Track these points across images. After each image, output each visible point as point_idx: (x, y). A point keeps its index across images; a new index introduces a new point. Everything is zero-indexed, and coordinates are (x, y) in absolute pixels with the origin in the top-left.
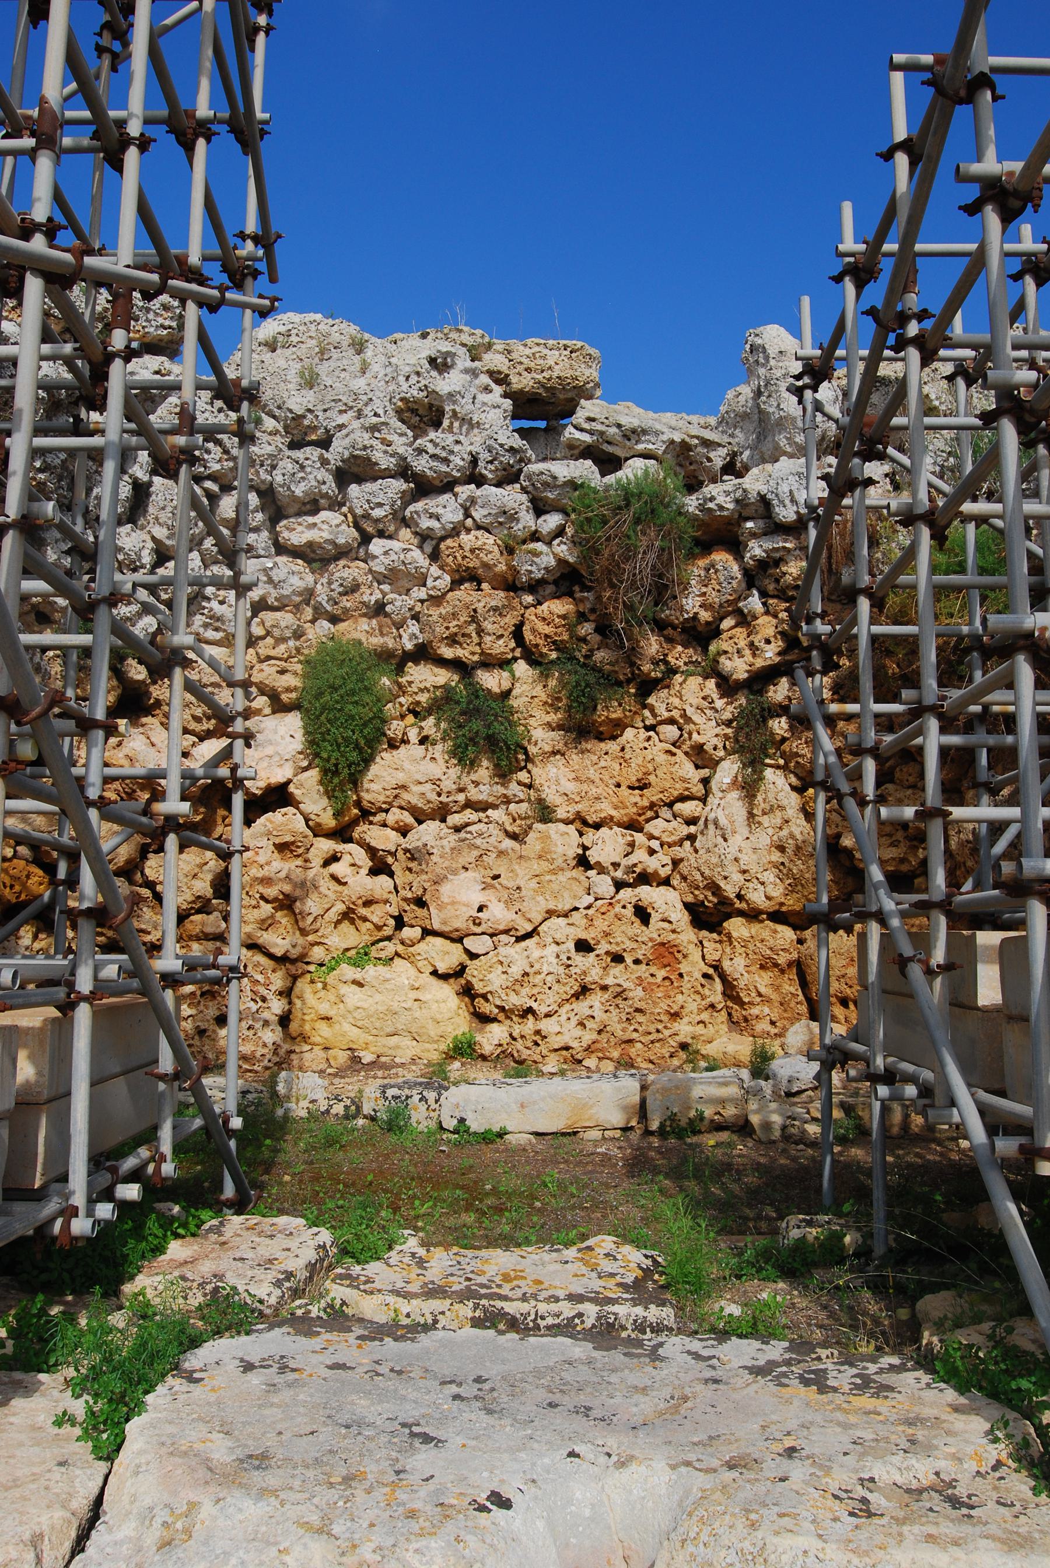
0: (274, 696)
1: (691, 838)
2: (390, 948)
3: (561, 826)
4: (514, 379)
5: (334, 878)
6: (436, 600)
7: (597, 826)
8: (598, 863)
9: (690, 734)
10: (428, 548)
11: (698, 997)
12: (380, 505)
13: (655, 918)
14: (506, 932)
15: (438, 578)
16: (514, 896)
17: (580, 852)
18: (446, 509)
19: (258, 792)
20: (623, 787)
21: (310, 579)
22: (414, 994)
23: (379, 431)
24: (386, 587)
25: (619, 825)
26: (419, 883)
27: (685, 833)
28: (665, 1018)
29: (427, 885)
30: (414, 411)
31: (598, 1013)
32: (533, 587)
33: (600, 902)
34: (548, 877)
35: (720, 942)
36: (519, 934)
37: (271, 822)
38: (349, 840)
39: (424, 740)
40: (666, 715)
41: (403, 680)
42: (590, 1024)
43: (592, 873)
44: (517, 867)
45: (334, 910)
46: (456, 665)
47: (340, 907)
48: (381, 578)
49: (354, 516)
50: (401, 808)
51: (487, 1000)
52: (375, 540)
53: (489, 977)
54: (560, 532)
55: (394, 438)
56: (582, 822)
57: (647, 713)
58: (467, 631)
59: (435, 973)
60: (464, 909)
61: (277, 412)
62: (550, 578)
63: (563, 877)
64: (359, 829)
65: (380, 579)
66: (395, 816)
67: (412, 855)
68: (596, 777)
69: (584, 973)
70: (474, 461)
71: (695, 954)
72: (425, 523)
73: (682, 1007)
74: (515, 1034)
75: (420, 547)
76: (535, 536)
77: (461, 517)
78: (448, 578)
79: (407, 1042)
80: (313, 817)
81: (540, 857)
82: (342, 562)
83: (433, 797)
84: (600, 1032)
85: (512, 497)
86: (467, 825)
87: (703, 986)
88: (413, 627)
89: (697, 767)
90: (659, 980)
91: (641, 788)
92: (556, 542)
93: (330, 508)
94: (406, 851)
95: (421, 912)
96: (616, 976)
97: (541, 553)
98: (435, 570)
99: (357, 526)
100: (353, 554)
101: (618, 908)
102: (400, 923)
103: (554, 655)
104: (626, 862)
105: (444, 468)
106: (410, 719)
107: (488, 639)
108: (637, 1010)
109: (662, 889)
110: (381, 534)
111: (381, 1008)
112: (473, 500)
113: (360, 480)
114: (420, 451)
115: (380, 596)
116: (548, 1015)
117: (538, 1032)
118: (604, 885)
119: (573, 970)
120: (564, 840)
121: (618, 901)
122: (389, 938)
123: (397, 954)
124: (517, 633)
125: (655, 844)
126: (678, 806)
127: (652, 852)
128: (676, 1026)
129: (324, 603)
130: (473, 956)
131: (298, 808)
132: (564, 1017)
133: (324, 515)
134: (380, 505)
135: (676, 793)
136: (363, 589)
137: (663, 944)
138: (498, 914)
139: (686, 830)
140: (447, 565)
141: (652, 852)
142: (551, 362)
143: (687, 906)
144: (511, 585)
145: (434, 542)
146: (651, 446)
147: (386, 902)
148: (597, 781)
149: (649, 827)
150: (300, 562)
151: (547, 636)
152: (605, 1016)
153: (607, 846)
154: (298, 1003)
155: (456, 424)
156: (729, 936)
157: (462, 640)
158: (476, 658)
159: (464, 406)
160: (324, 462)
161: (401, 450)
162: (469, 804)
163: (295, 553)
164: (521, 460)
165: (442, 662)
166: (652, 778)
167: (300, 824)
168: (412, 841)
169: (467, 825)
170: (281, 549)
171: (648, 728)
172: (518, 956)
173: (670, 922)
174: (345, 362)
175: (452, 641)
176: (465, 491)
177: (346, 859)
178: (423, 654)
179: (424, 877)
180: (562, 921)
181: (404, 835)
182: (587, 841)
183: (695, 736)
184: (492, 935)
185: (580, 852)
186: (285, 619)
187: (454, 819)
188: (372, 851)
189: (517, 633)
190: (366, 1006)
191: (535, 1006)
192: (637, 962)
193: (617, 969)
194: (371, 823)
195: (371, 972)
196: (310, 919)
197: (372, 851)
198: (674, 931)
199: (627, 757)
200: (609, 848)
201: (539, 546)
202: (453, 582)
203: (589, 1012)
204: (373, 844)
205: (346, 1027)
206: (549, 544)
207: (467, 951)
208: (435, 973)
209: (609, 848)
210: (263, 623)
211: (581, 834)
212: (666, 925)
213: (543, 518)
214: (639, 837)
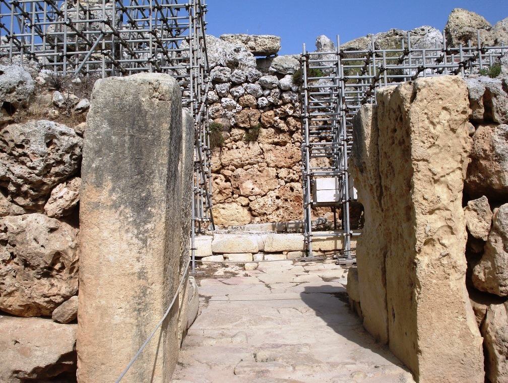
2: (231, 200)
5: (216, 183)
6: (238, 113)
7: (281, 168)
8: (281, 177)
10: (236, 99)
12: (224, 90)
14: (259, 195)
16: (260, 186)
18: (240, 90)
22: (237, 211)
24: (226, 110)
26: (237, 183)
28: (298, 214)
31: (282, 214)
32: (263, 108)
38: (220, 174)
39: (237, 148)
41: (231, 133)
43: (280, 180)
46: (244, 128)
47: (218, 190)
50: (232, 165)
53: (255, 206)
54: (269, 94)
55: (227, 72)
56: (277, 167)
57: (292, 139)
64: (222, 171)
65: (224, 108)
66: (231, 167)
67: (235, 177)
68: (279, 155)
70: (247, 77)
72: (235, 94)
75: (234, 99)
76: (263, 95)
79: (235, 222)
82: (215, 104)
83: (240, 162)
84: (282, 218)
85: (256, 86)
86: (249, 169)
88: (233, 119)
94: (234, 176)
95: (238, 191)
96: (287, 205)
98: (238, 105)
99: (218, 95)
101: (286, 188)
102: (233, 194)
103: (269, 125)
106: (233, 142)
107: (252, 122)
108: (291, 212)
110: (224, 97)
112: (247, 87)
114: (233, 76)
116: (269, 214)
117: (267, 218)
118: (283, 182)
120: (273, 172)
122: (230, 197)
123: (232, 201)
124: (259, 120)
125: (295, 172)
127: (294, 174)
128: (300, 216)
130: (251, 201)
132: (273, 215)
134: (224, 90)
136: (220, 111)
138: (257, 190)
142: (266, 43)
144: (257, 107)
147: (229, 188)
149: (294, 168)
151: (267, 121)
152: (283, 214)
153: (283, 173)
155: (242, 66)
158: (249, 127)
159: (244, 61)
161: (228, 76)
162: (249, 164)
165: (241, 128)
168: (235, 173)
169: (249, 169)
171: (293, 143)
172: (261, 200)
175: (243, 122)
176: (245, 85)
177: (219, 178)
178: (236, 126)
180: (273, 192)
187: (245, 167)
188: (225, 176)
189: (259, 120)
191: (266, 212)
193: (287, 203)
194: (225, 169)
195: (226, 205)
197: (225, 176)
201: (264, 98)
204: (226, 174)
205: (221, 219)
206: (266, 97)
207: (250, 200)
208: (242, 205)
214: (291, 170)
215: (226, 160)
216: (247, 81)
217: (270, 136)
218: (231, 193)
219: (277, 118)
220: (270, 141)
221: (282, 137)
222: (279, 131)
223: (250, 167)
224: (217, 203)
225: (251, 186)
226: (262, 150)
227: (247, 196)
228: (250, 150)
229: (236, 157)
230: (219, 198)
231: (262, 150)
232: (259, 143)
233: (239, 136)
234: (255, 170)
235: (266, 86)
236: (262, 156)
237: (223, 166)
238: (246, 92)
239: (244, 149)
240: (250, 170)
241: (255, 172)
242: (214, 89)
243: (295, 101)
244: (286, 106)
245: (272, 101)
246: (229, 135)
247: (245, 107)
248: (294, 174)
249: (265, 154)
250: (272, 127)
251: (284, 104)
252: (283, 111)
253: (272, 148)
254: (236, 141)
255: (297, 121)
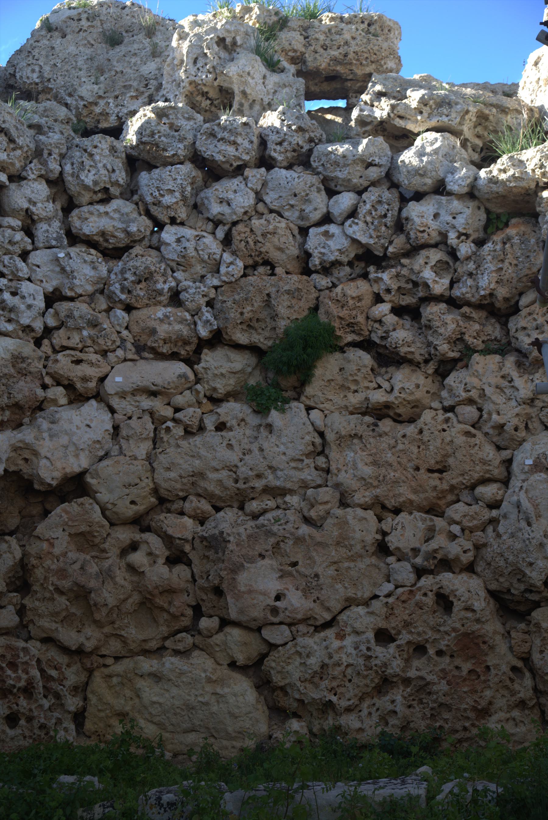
0: (70, 387)
1: (494, 521)
3: (359, 511)
4: (309, 57)
5: (132, 568)
7: (397, 511)
8: (398, 549)
9: (490, 414)
10: (221, 233)
11: (506, 693)
12: (171, 192)
13: (457, 606)
14: (305, 620)
15: (231, 263)
16: (311, 586)
17: (379, 537)
19: (54, 483)
20: (422, 471)
21: (103, 269)
23: (167, 116)
25: (420, 509)
27: (487, 517)
29: (223, 573)
30: (205, 94)
31: (399, 708)
32: (326, 269)
33: (400, 590)
34: (346, 564)
35: (527, 632)
36: (318, 623)
37: (67, 512)
38: (147, 529)
39: (221, 427)
40: (464, 395)
42: (393, 721)
43: (391, 559)
44: (314, 554)
45: (130, 601)
48: (174, 264)
49: (146, 204)
50: (199, 495)
51: (286, 694)
52: (167, 228)
53: (288, 670)
54: (353, 214)
55: (182, 122)
58: (261, 316)
59: (233, 665)
60: (261, 598)
61: (69, 100)
62: (345, 259)
63: (361, 565)
66: (194, 504)
69: (385, 665)
71: (502, 647)
72: (215, 209)
73: (490, 703)
74: (315, 730)
76: (327, 219)
77: (252, 201)
78: (240, 264)
80: (110, 506)
81: (338, 543)
83: (230, 483)
87: (512, 680)
88: (207, 315)
89: (499, 448)
90: (464, 673)
91: (440, 471)
92: (348, 223)
93: (122, 196)
94: (203, 539)
96: (418, 668)
97: (333, 235)
98: (227, 257)
99: (148, 214)
100: (146, 242)
102: (198, 611)
103: (350, 338)
104: (425, 548)
105: (231, 150)
106: (208, 405)
109: (464, 576)
110: (173, 221)
111: (177, 703)
113: (150, 167)
115: (173, 284)
116: (349, 710)
118: (404, 572)
119: (374, 662)
120: (363, 527)
121: (420, 589)
122: (185, 630)
125: (456, 529)
126: (480, 490)
129: (118, 292)
130: (273, 646)
131: (95, 499)
132: (365, 712)
133: (116, 203)
134: (171, 192)
135: (476, 476)
137: (466, 635)
138: (296, 602)
139: (488, 514)
140: (239, 250)
141: (453, 537)
143: (492, 594)
145: (226, 228)
146: (445, 119)
148: (395, 464)
150: (93, 251)
152: (408, 712)
153: (407, 531)
154: (93, 700)
156: (538, 625)
157: (256, 325)
160: (113, 150)
162: (269, 491)
163: (90, 243)
164: (311, 140)
165: (237, 347)
166: (451, 461)
167: (97, 514)
168: (210, 529)
169: (264, 512)
170: (73, 238)
172: (317, 647)
173: (473, 611)
174: (136, 46)
176: (255, 175)
177: (144, 548)
178: (217, 339)
179: (221, 565)
180: (361, 610)
181: (202, 523)
182: (385, 526)
183: (495, 416)
184: (290, 625)
185: (379, 537)
186: (81, 309)
187: (254, 506)
190: (161, 700)
191: (334, 699)
192: (440, 653)
194: (169, 511)
196: (104, 611)
197: (168, 540)
198: (478, 621)
199: (425, 439)
200: (409, 533)
202: (246, 267)
203: (391, 707)
204: (170, 531)
208: (233, 665)
209: (409, 533)
210: (57, 314)
211: (380, 520)
212: (470, 615)
213: (335, 198)
214: (439, 522)
215: (173, 475)
216: (266, 162)
217: (356, 382)
218: (189, 612)
219: (384, 308)
220: (355, 400)
221: (407, 383)
222: (388, 359)
223: (271, 504)
224: (133, 654)
225: (271, 584)
226: (321, 434)
227: (256, 629)
228: (273, 439)
229: (214, 464)
230: (134, 633)
231: (321, 434)
232: (309, 409)
233: (232, 382)
234: (291, 516)
235: (341, 174)
236: (321, 461)
237: (163, 501)
238: (261, 207)
239: (248, 432)
240: (269, 516)
241: (289, 527)
242: (133, 192)
243: (460, 235)
244: (420, 260)
245: (364, 240)
246: (192, 377)
247: (254, 267)
248: (453, 537)
249: (333, 453)
250: (366, 345)
251: (413, 250)
252: (409, 281)
253: (361, 430)
254: (216, 401)
255: (467, 318)
